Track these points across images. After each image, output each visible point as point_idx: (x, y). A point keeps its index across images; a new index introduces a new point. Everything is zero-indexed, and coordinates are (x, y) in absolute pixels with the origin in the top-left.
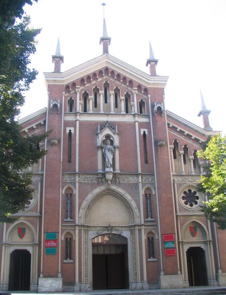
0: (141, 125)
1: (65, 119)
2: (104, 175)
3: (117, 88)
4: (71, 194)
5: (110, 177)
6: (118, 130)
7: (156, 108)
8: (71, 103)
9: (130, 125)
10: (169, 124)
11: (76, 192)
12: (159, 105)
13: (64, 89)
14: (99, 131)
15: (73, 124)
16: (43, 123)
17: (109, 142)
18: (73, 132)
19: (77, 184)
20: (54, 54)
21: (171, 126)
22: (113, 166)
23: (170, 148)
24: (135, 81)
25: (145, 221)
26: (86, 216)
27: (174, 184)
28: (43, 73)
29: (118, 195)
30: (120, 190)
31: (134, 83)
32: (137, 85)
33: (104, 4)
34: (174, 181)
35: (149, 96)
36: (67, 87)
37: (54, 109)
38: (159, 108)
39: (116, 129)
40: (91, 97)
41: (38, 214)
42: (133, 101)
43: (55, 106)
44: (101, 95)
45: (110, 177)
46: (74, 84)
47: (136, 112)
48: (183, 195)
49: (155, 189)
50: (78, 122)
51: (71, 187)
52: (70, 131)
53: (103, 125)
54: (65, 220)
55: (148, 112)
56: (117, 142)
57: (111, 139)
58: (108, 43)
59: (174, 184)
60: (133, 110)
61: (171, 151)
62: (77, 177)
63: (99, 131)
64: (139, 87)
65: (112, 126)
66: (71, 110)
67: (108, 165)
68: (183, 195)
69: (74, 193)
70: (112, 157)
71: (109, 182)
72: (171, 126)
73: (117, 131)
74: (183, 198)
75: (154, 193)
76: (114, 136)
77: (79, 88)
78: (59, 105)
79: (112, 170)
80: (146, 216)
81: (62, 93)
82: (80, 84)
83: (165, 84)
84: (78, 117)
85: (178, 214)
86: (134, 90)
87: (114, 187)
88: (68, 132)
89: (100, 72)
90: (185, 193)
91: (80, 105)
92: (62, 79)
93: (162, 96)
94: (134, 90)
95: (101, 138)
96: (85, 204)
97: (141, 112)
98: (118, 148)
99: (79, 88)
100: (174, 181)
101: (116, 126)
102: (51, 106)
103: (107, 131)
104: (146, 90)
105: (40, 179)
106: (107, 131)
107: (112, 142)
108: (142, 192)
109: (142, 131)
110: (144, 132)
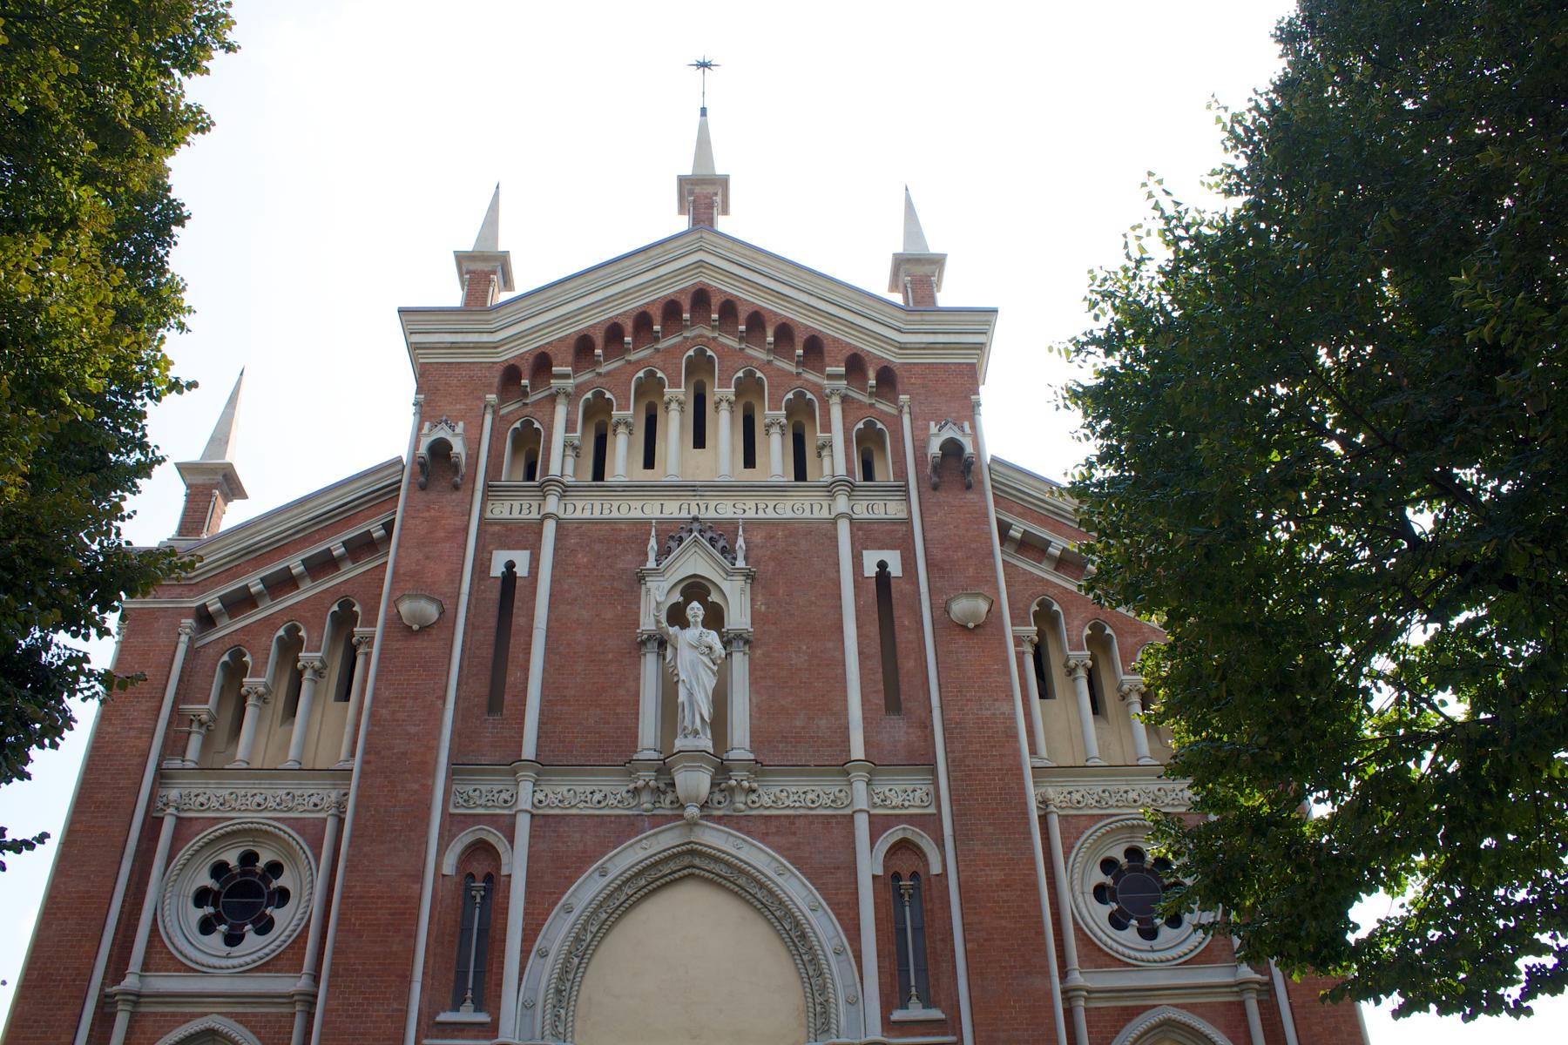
0: (866, 535)
1: (488, 515)
2: (664, 769)
3: (750, 374)
4: (490, 878)
5: (695, 782)
6: (746, 558)
7: (934, 448)
8: (529, 446)
9: (810, 533)
10: (1004, 528)
11: (516, 865)
12: (948, 433)
13: (496, 381)
14: (651, 564)
15: (526, 535)
16: (378, 533)
17: (695, 610)
18: (521, 570)
19: (523, 826)
20: (468, 246)
21: (1016, 533)
22: (719, 723)
23: (1018, 641)
24: (836, 340)
25: (888, 1025)
26: (559, 991)
27: (1044, 820)
28: (401, 311)
29: (742, 881)
30: (758, 857)
31: (828, 347)
32: (847, 353)
33: (704, 65)
34: (1044, 802)
35: (904, 398)
36: (511, 375)
37: (435, 463)
38: (952, 449)
39: (740, 555)
40: (627, 412)
41: (301, 983)
42: (827, 427)
43: (440, 450)
44: (674, 406)
45: (695, 782)
46: (543, 363)
47: (841, 470)
48: (1099, 877)
49: (940, 843)
50: (549, 529)
51: (491, 839)
52: (510, 565)
53: (672, 536)
54: (444, 1017)
55: (901, 474)
56: (738, 616)
57: (714, 597)
58: (718, 199)
59: (1044, 820)
60: (827, 470)
61: (1020, 657)
62: (526, 788)
63: (651, 564)
64: (855, 364)
65: (720, 536)
66: (530, 475)
67: (687, 722)
68: (1099, 877)
69: (504, 872)
70: (710, 682)
71: (692, 811)
72: (1016, 533)
73: (740, 563)
74: (1100, 893)
75: (935, 869)
76: (726, 586)
77: (566, 376)
78: (458, 447)
79: (706, 742)
80: (894, 994)
81: (482, 398)
82: (570, 358)
83: (981, 347)
84: (552, 504)
85: (1077, 978)
86: (831, 377)
87: (715, 838)
88: (497, 570)
89: (671, 309)
90: (1108, 865)
91: (569, 452)
92: (485, 338)
93: (967, 398)
94: (831, 377)
95: (659, 593)
96: (558, 932)
97: (868, 474)
98: (747, 642)
99: (566, 376)
100: (1044, 802)
101: (740, 541)
102: (423, 450)
103: (694, 562)
104: (887, 380)
105: (334, 795)
106: (694, 562)
107: (714, 618)
108: (869, 864)
109: (871, 561)
110: (882, 565)
